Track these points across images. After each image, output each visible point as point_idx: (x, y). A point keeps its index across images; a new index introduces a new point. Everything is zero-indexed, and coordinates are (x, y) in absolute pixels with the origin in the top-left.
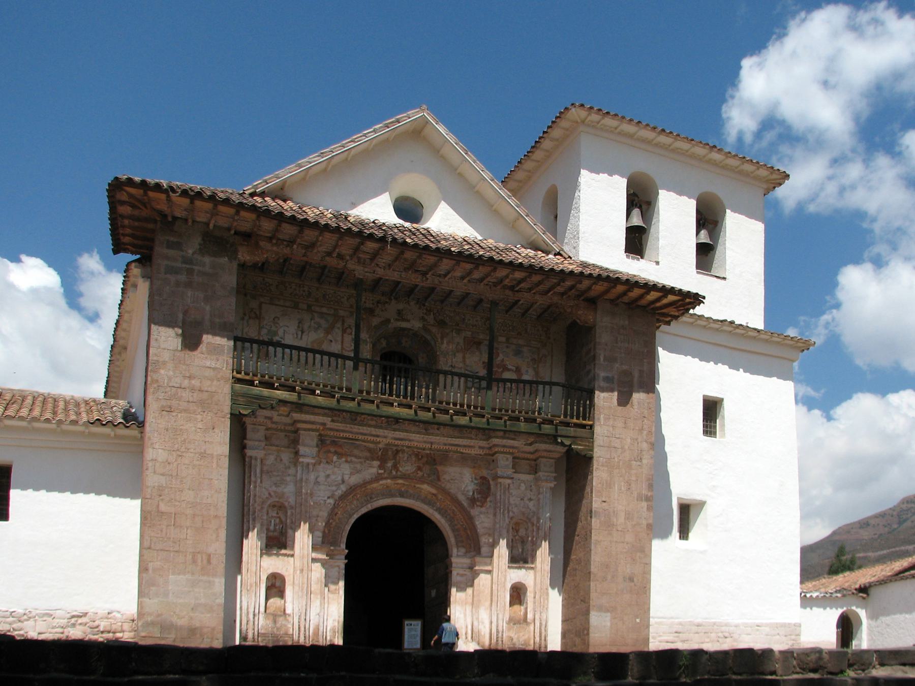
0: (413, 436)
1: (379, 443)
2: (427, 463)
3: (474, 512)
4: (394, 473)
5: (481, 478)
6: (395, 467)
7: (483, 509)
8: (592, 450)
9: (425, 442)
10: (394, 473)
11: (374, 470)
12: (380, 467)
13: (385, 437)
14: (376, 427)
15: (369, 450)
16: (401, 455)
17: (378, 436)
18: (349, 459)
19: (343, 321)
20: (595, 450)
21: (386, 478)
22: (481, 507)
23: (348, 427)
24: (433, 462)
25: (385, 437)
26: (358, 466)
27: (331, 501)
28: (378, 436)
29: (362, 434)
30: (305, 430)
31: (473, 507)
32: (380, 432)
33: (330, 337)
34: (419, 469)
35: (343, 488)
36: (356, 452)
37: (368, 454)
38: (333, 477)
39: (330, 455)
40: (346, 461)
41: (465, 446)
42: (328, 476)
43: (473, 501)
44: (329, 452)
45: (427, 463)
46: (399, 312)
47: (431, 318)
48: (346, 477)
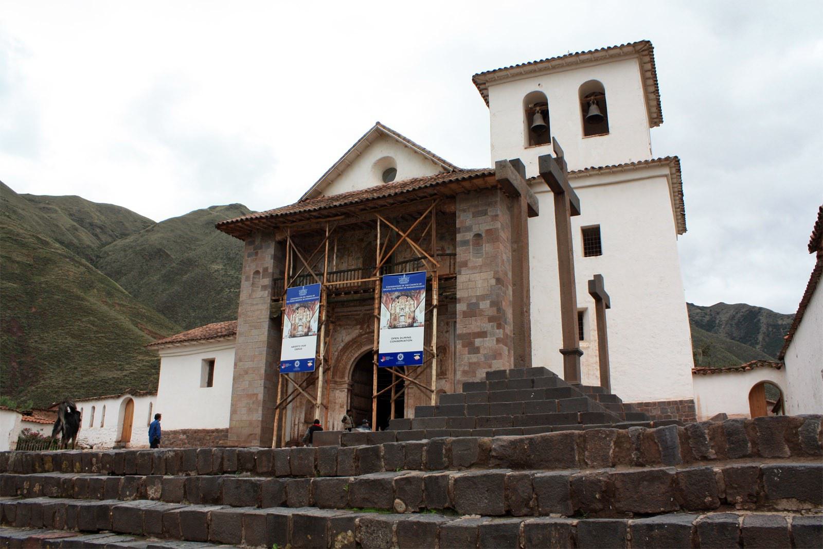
1: (359, 314)
4: (368, 330)
8: (456, 294)
12: (361, 328)
14: (354, 306)
15: (356, 320)
17: (357, 311)
18: (345, 327)
20: (458, 293)
21: (364, 334)
25: (361, 311)
28: (357, 311)
29: (350, 311)
32: (358, 308)
33: (342, 261)
37: (355, 322)
40: (344, 329)
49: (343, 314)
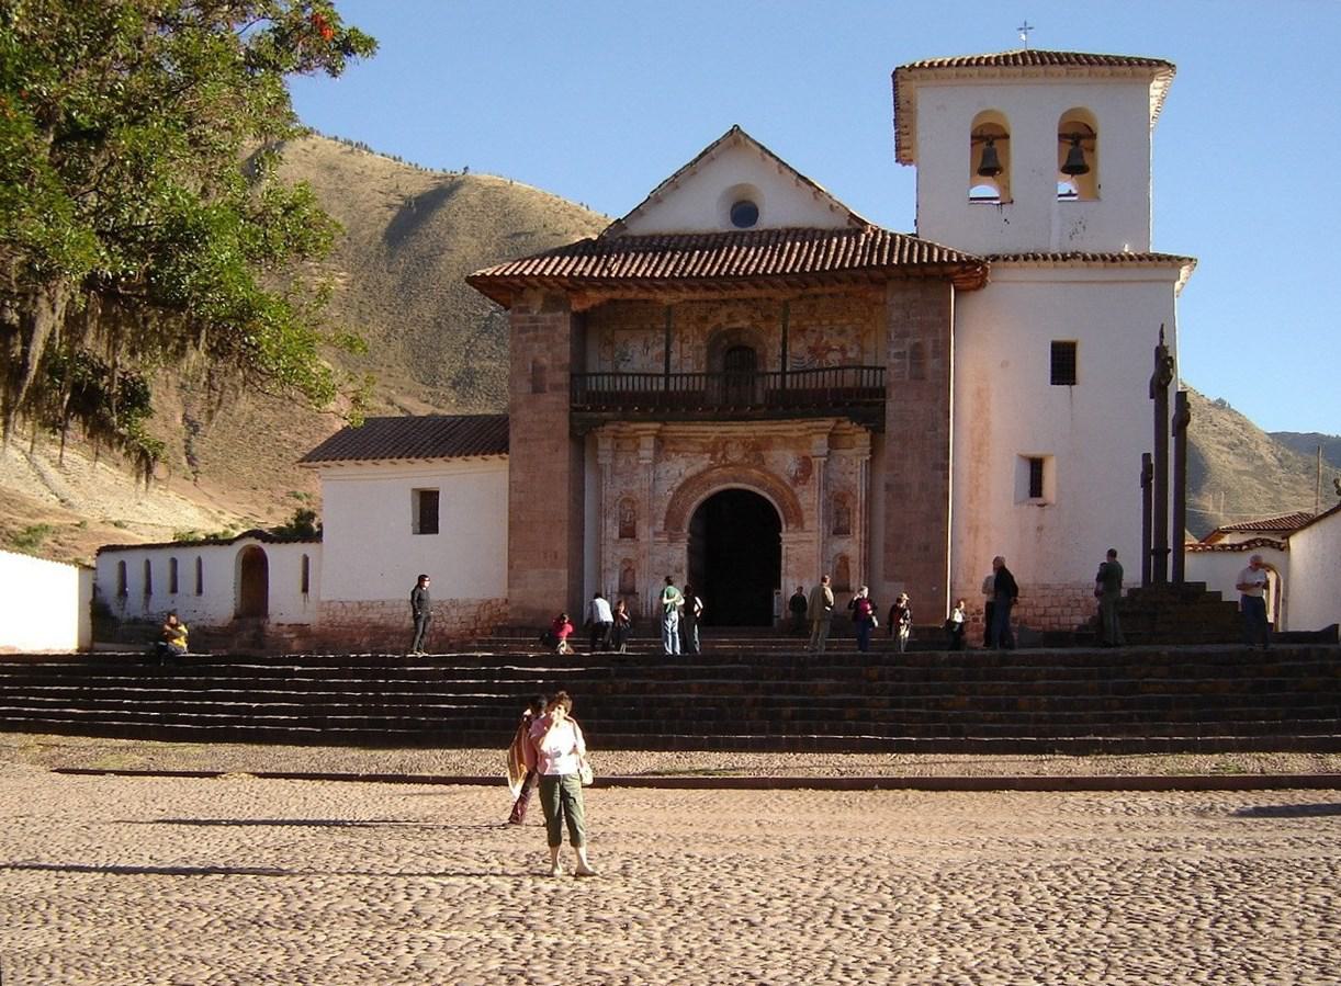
0: (735, 428)
1: (708, 437)
2: (753, 449)
3: (797, 490)
5: (804, 457)
6: (724, 457)
7: (805, 487)
9: (749, 432)
10: (723, 462)
11: (705, 462)
12: (711, 459)
13: (712, 432)
15: (702, 444)
16: (729, 445)
19: (681, 333)
22: (804, 484)
23: (681, 428)
24: (757, 449)
25: (712, 432)
26: (693, 461)
27: (671, 493)
28: (706, 432)
30: (645, 435)
31: (796, 486)
34: (746, 456)
35: (681, 481)
36: (691, 448)
37: (700, 448)
38: (672, 472)
39: (669, 453)
41: (785, 431)
42: (668, 471)
43: (796, 480)
44: (667, 451)
45: (753, 449)
46: (729, 315)
47: (758, 316)
48: (683, 471)
49: (681, 434)
